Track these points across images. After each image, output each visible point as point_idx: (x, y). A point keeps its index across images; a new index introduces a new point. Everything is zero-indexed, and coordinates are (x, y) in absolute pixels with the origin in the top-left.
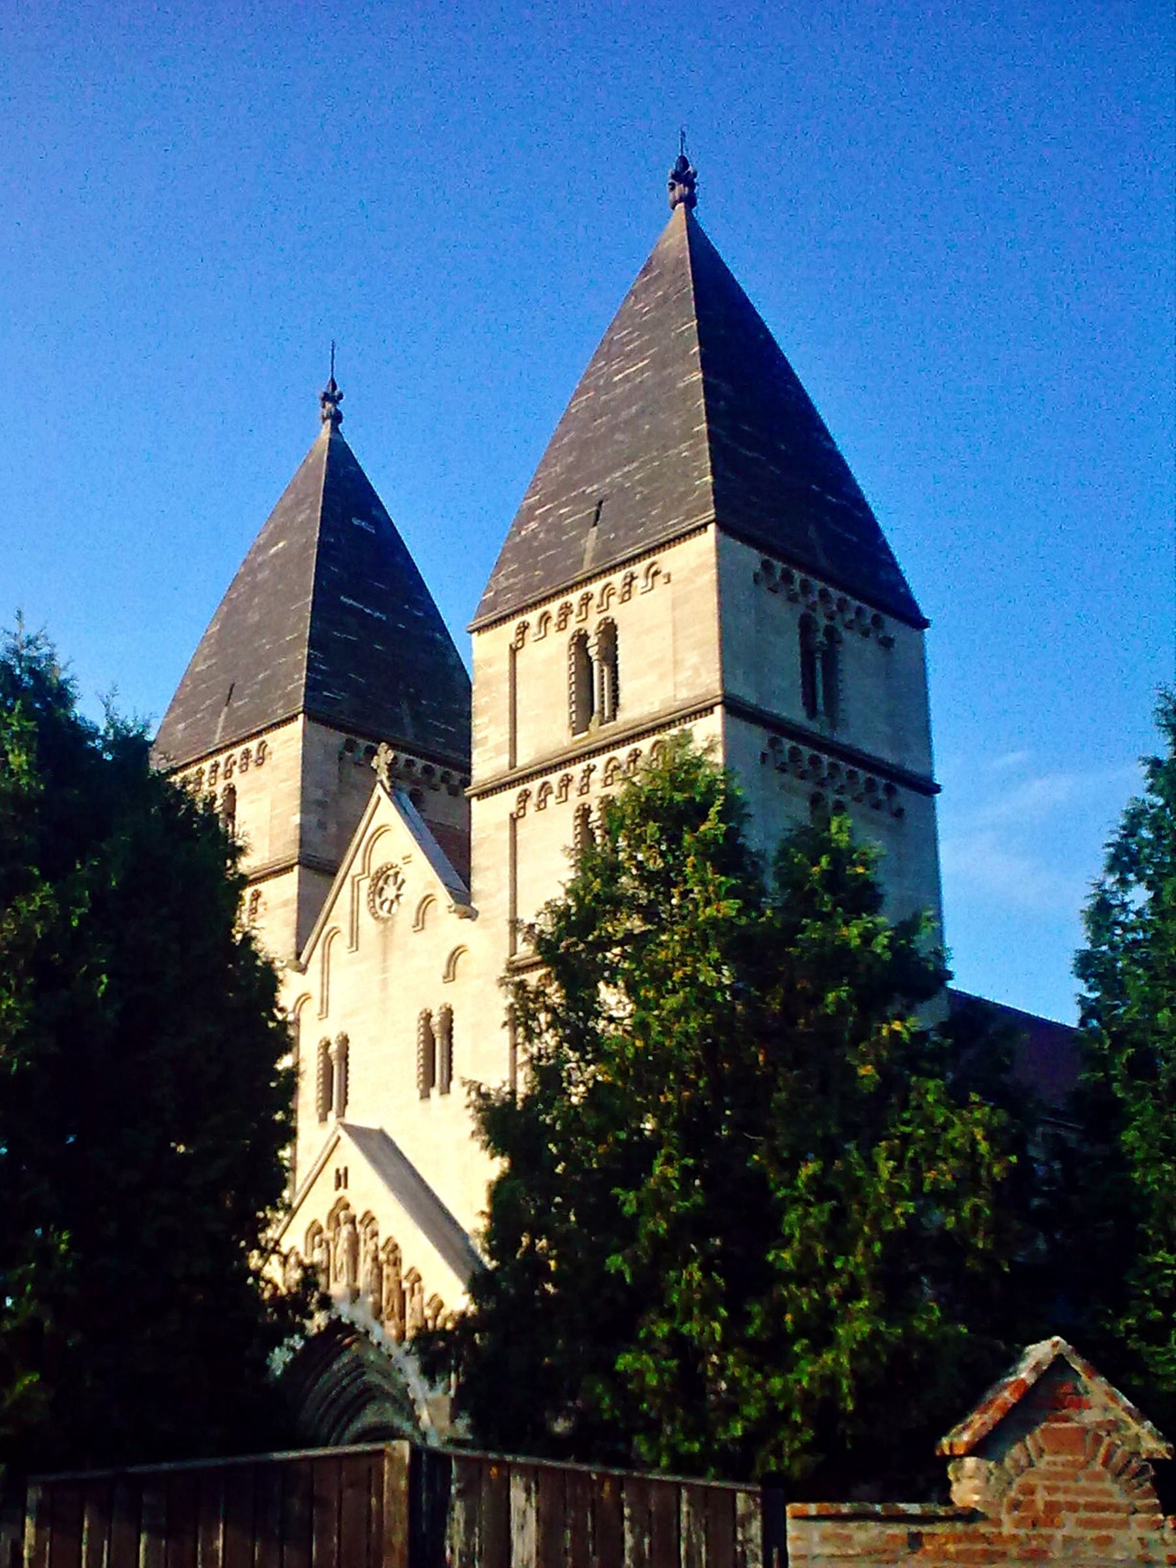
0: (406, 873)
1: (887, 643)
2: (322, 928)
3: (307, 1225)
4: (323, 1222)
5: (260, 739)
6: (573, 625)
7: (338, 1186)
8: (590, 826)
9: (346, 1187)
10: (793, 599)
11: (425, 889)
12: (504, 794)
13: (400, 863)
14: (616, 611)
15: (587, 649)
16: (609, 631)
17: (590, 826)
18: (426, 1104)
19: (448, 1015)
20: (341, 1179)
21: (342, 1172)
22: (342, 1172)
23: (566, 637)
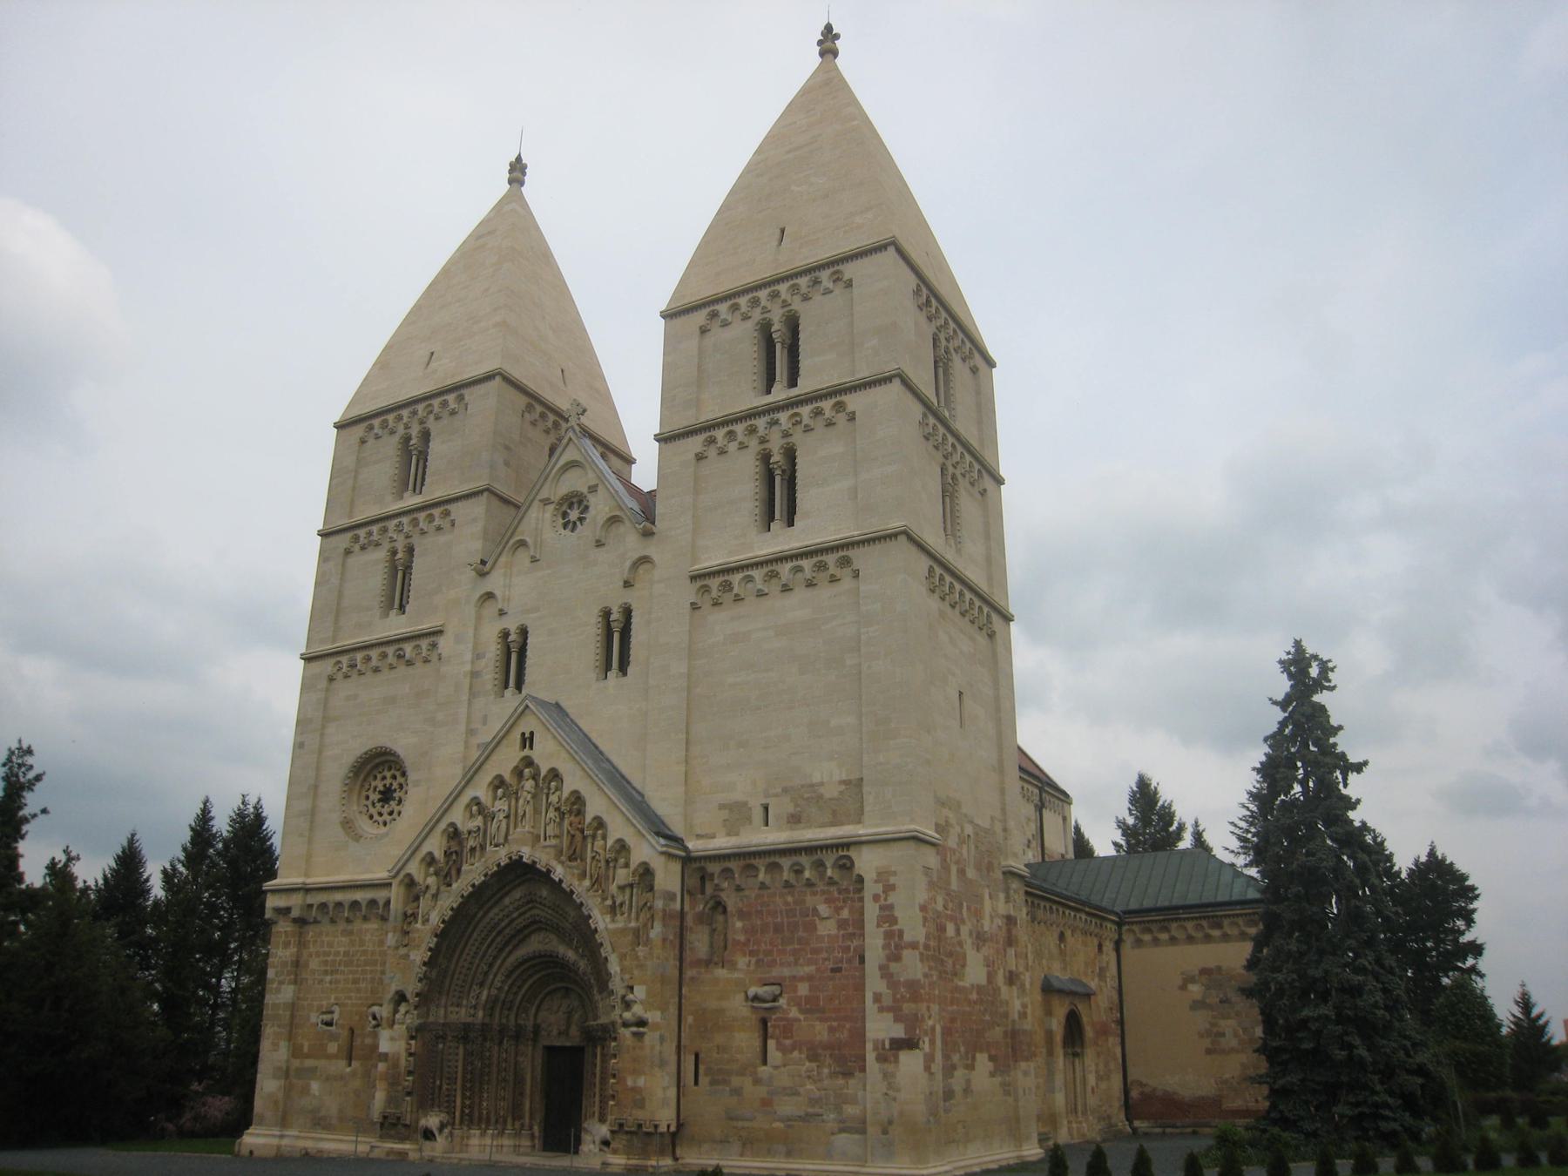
0: (593, 500)
1: (974, 370)
2: (511, 537)
3: (489, 779)
4: (507, 777)
5: (459, 393)
6: (757, 315)
7: (524, 747)
8: (771, 466)
9: (531, 747)
10: (930, 319)
11: (610, 512)
12: (690, 440)
13: (585, 490)
14: (797, 305)
15: (771, 335)
16: (793, 325)
17: (771, 466)
18: (602, 684)
19: (627, 612)
20: (528, 741)
21: (527, 735)
22: (527, 735)
23: (750, 324)
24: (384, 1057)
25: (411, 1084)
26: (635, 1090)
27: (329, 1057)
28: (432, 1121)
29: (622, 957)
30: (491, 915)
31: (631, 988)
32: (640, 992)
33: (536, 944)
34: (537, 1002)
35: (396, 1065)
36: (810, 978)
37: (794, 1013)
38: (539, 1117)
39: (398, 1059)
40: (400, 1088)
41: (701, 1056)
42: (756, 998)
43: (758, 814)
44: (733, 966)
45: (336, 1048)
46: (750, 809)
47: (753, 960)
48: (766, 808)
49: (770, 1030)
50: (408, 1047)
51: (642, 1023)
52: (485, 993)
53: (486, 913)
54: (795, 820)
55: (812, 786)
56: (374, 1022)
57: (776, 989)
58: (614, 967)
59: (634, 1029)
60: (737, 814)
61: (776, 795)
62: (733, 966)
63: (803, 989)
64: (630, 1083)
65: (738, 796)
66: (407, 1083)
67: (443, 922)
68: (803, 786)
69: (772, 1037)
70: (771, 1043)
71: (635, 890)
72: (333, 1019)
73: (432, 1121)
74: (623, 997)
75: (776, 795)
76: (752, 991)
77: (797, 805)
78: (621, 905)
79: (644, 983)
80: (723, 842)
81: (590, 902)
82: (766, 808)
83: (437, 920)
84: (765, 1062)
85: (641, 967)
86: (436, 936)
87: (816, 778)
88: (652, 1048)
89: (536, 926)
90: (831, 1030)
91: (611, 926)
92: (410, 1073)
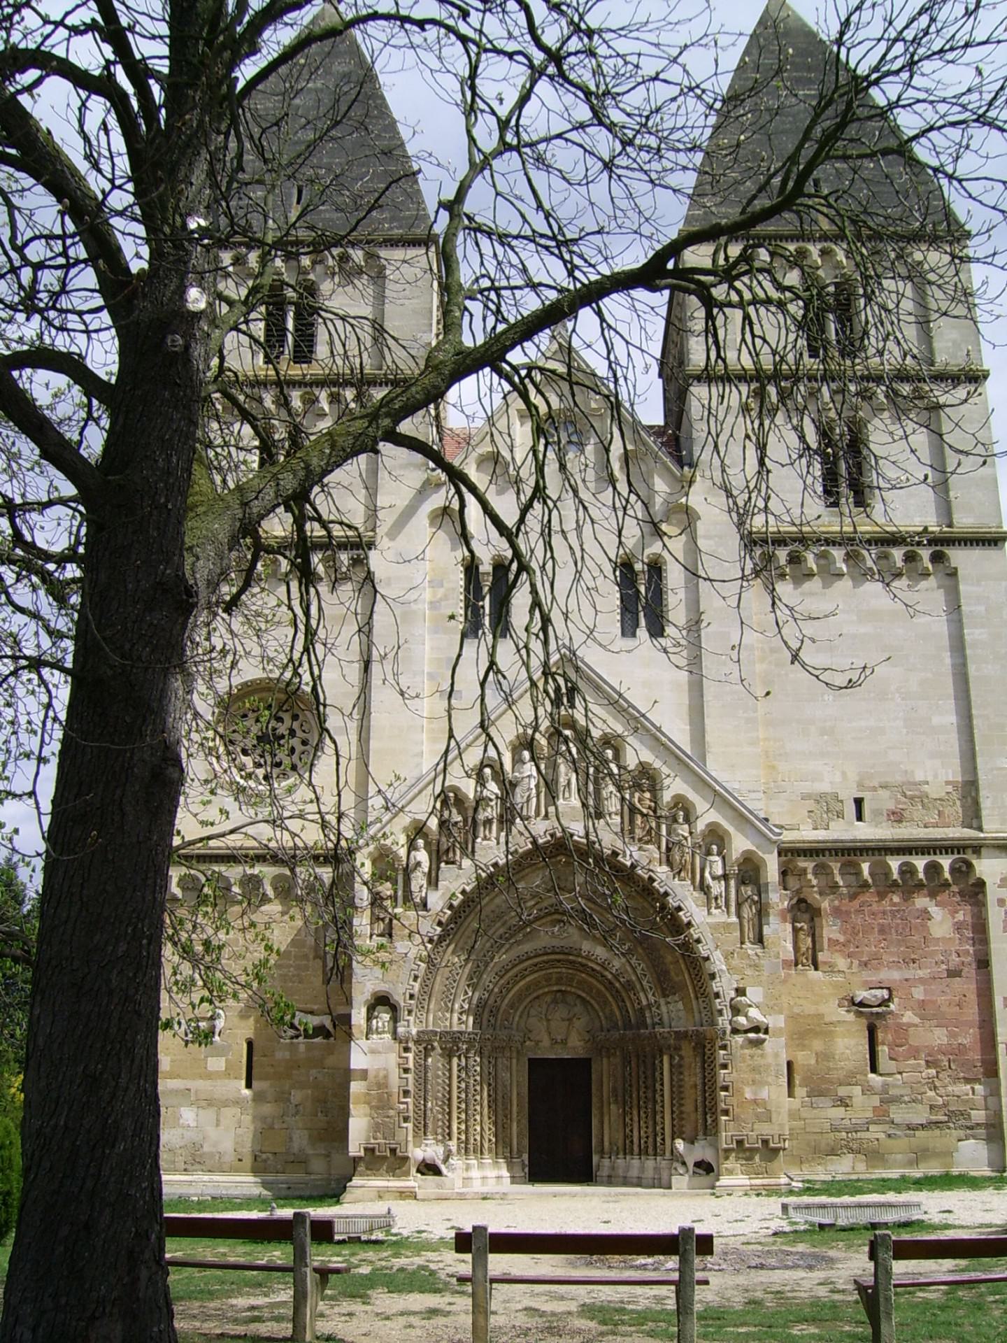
24: (364, 1074)
25: (411, 1107)
26: (755, 1101)
27: (209, 1076)
28: (430, 1150)
29: (728, 956)
30: (497, 901)
31: (740, 992)
32: (754, 994)
33: (547, 937)
34: (521, 1009)
35: (382, 1084)
36: (922, 981)
37: (909, 1017)
38: (526, 1142)
39: (386, 1077)
40: (392, 1113)
41: (796, 1066)
42: (861, 1004)
43: (850, 809)
44: (832, 969)
45: (223, 1065)
46: (842, 801)
47: (856, 962)
48: (859, 802)
49: (880, 1035)
50: (401, 1061)
51: (756, 1029)
52: (477, 995)
53: (492, 900)
54: (897, 817)
55: (915, 784)
56: (291, 1032)
57: (885, 993)
58: (718, 963)
59: (751, 1035)
60: (827, 805)
61: (874, 789)
62: (832, 969)
63: (918, 993)
64: (748, 1094)
65: (824, 787)
66: (402, 1106)
67: (451, 907)
68: (904, 783)
69: (883, 1044)
70: (883, 1050)
71: (732, 883)
72: (214, 1027)
73: (430, 1150)
74: (732, 999)
75: (874, 789)
76: (861, 995)
77: (898, 802)
78: (716, 898)
79: (760, 984)
80: (808, 834)
81: (678, 891)
82: (859, 802)
83: (441, 904)
84: (874, 1069)
85: (756, 967)
86: (440, 924)
87: (919, 776)
88: (776, 1055)
89: (556, 914)
90: (952, 1035)
91: (710, 920)
92: (406, 1093)
